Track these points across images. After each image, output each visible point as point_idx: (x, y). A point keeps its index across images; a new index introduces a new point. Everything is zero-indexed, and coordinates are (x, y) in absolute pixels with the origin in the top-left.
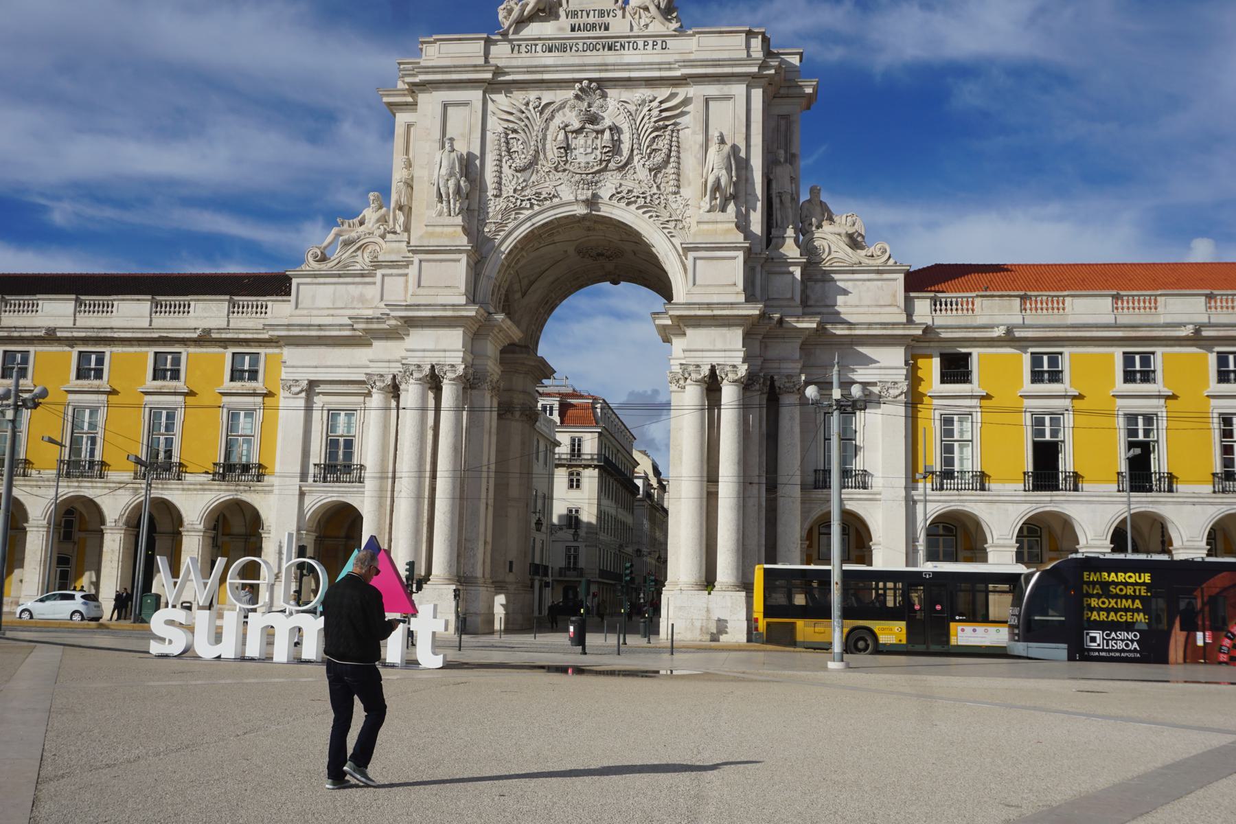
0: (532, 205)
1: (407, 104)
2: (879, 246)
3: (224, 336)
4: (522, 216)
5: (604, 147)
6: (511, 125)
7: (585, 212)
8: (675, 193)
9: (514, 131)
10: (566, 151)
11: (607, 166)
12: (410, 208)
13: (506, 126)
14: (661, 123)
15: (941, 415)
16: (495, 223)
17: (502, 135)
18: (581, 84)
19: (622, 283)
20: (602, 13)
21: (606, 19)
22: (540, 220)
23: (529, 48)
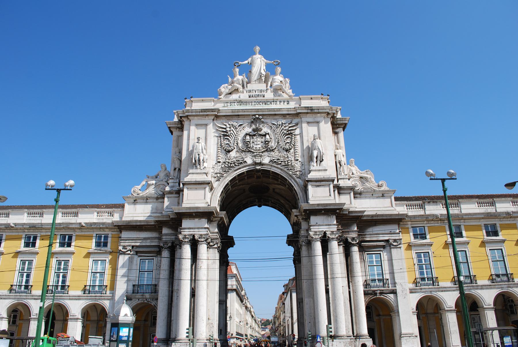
2: (382, 182)
3: (93, 226)
5: (267, 141)
6: (225, 133)
9: (226, 135)
11: (267, 149)
12: (180, 170)
13: (223, 133)
14: (290, 132)
15: (416, 253)
16: (219, 173)
17: (221, 137)
19: (264, 207)
21: (263, 93)
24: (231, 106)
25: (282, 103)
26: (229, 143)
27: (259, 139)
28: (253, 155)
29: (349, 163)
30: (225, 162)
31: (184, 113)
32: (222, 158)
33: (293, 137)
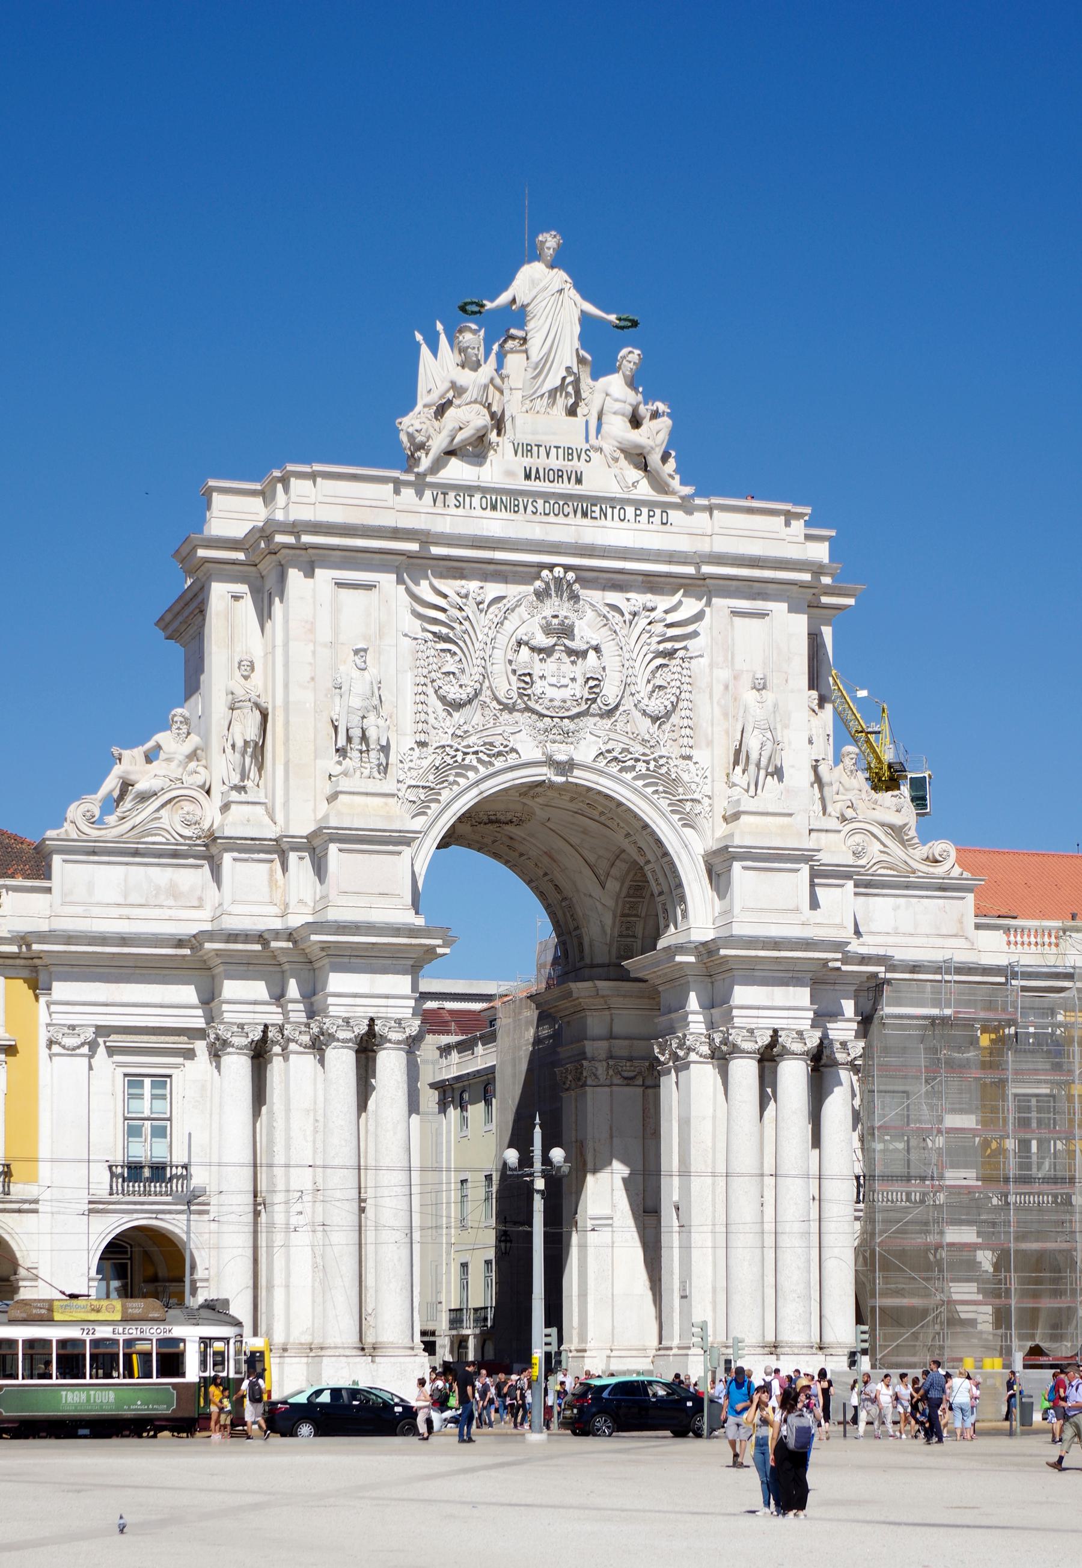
0: (479, 760)
1: (234, 563)
2: (943, 846)
4: (460, 780)
5: (588, 679)
6: (445, 630)
7: (563, 779)
8: (689, 758)
9: (447, 639)
10: (531, 679)
13: (435, 628)
14: (669, 645)
16: (424, 787)
18: (551, 571)
20: (569, 453)
22: (492, 786)
23: (461, 499)
24: (460, 511)
25: (644, 518)
26: (456, 671)
27: (564, 668)
28: (540, 725)
29: (838, 759)
30: (444, 747)
31: (297, 535)
32: (435, 728)
33: (679, 669)
